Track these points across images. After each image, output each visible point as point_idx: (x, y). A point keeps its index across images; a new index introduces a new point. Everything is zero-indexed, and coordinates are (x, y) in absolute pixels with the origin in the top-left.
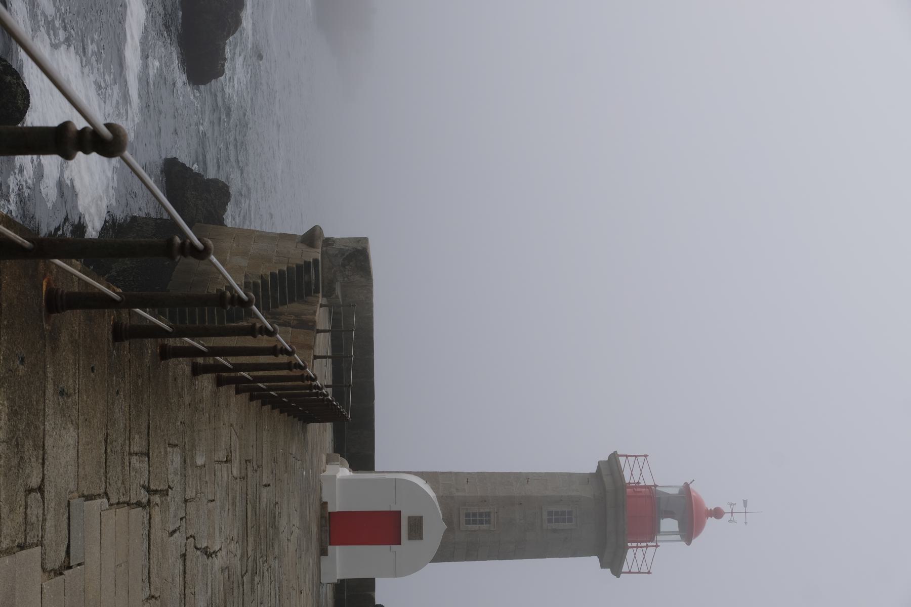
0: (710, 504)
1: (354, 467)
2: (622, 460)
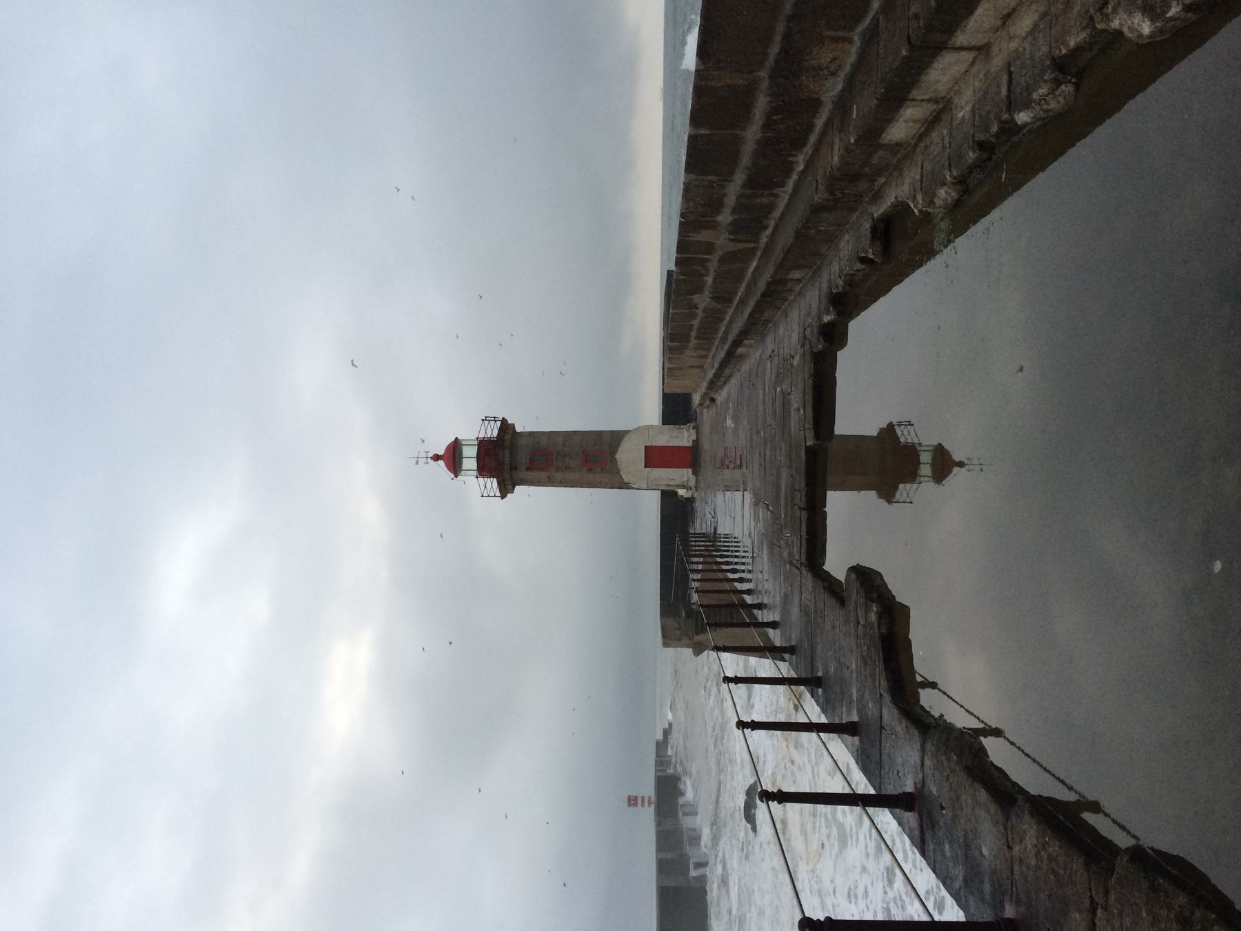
1: (675, 493)
2: (498, 494)
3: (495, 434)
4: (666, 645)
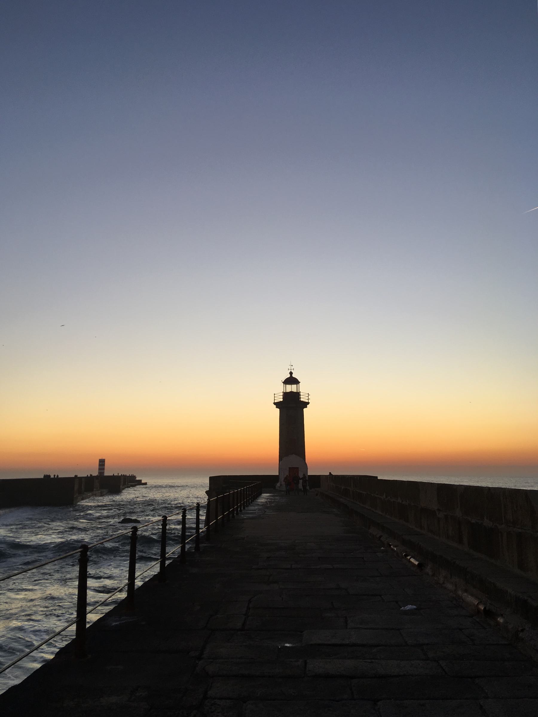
0: (289, 376)
1: (278, 482)
2: (276, 401)
3: (302, 400)
4: (210, 477)
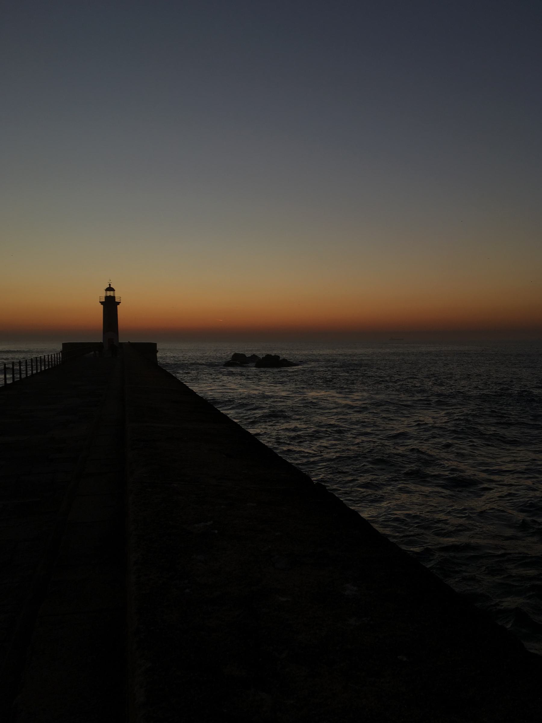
3: (116, 301)
